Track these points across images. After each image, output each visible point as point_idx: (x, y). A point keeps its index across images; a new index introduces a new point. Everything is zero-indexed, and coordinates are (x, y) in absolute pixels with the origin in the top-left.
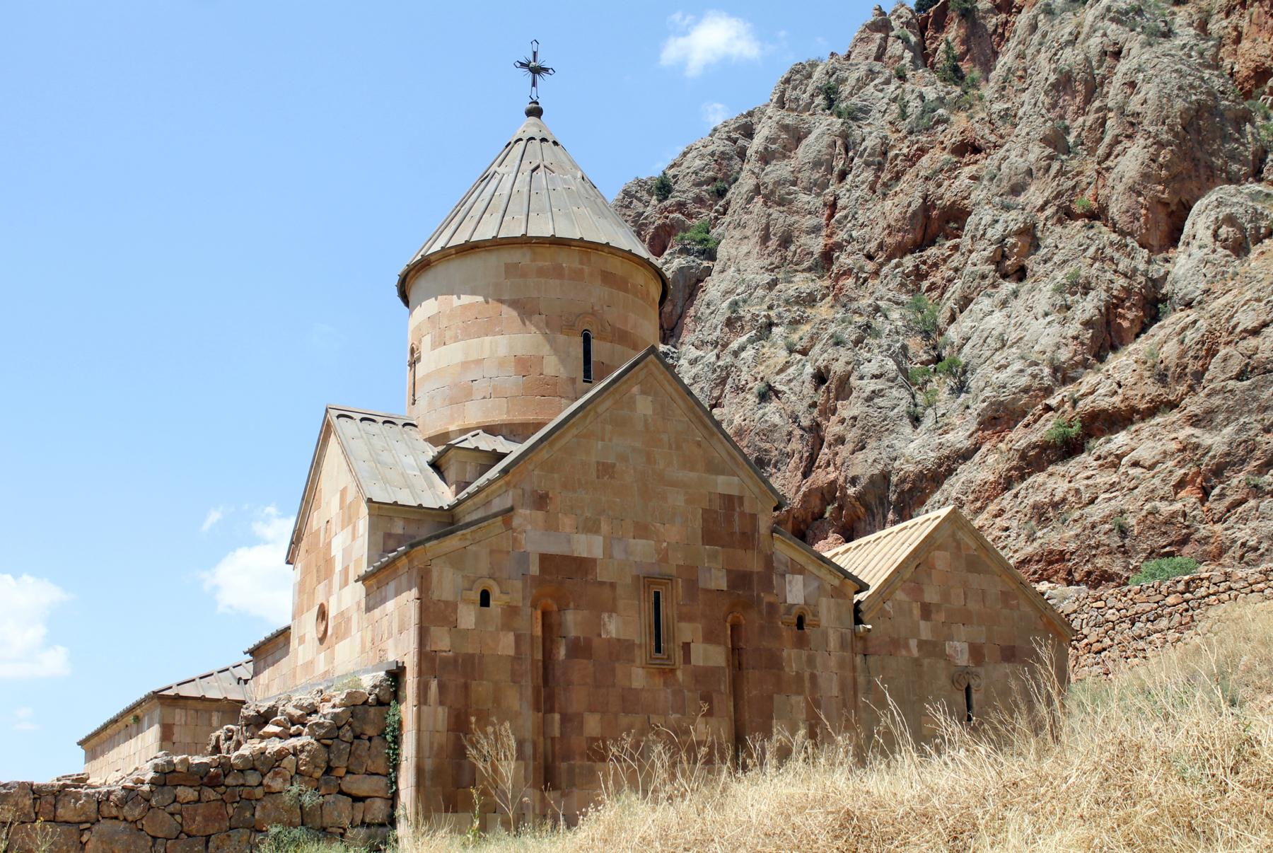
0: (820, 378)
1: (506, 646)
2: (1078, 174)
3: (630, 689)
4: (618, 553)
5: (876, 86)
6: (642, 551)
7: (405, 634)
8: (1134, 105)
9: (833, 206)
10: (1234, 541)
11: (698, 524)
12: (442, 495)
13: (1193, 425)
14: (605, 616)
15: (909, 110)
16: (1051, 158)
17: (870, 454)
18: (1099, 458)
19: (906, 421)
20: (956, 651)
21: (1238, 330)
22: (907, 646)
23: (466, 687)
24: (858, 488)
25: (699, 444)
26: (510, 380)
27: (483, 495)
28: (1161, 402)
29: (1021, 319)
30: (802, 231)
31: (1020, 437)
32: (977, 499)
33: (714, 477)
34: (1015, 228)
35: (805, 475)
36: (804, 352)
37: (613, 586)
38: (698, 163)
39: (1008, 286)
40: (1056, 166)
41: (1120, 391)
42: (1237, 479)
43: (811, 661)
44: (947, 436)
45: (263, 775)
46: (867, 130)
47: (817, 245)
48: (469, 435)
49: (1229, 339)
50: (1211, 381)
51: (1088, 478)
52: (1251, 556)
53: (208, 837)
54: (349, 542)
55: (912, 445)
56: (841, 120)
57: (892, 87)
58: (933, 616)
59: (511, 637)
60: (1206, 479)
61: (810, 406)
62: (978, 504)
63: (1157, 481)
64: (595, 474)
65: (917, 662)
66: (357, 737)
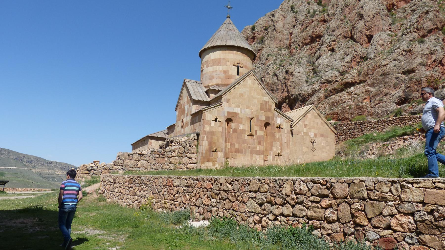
0: (287, 72)
1: (220, 129)
2: (348, 28)
3: (245, 139)
4: (243, 112)
5: (303, 6)
6: (248, 112)
7: (200, 126)
8: (362, 12)
9: (291, 34)
11: (259, 106)
12: (207, 99)
13: (369, 86)
14: (240, 124)
15: (310, 12)
16: (342, 24)
17: (297, 89)
18: (347, 92)
19: (305, 82)
20: (311, 134)
21: (381, 65)
22: (301, 133)
23: (212, 137)
24: (293, 97)
25: (260, 90)
26: (222, 75)
27: (216, 99)
28: (362, 81)
29: (332, 61)
30: (284, 39)
31: (330, 87)
32: (319, 100)
33: (263, 97)
34: (332, 40)
35: (282, 93)
36: (283, 66)
37: (242, 118)
38: (262, 23)
39: (330, 53)
40: (343, 26)
41: (353, 78)
42: (378, 98)
43: (281, 135)
44: (314, 86)
45: (172, 153)
46: (300, 16)
47: (287, 42)
48: (213, 86)
49: (379, 67)
50: (374, 76)
51: (344, 97)
52: (380, 115)
53: (161, 164)
54: (188, 107)
55: (306, 88)
56: (295, 14)
57: (306, 6)
58: (307, 127)
59: (221, 128)
60: (370, 98)
61: (284, 78)
62: (319, 101)
64: (239, 96)
65: (303, 136)
66: (190, 146)
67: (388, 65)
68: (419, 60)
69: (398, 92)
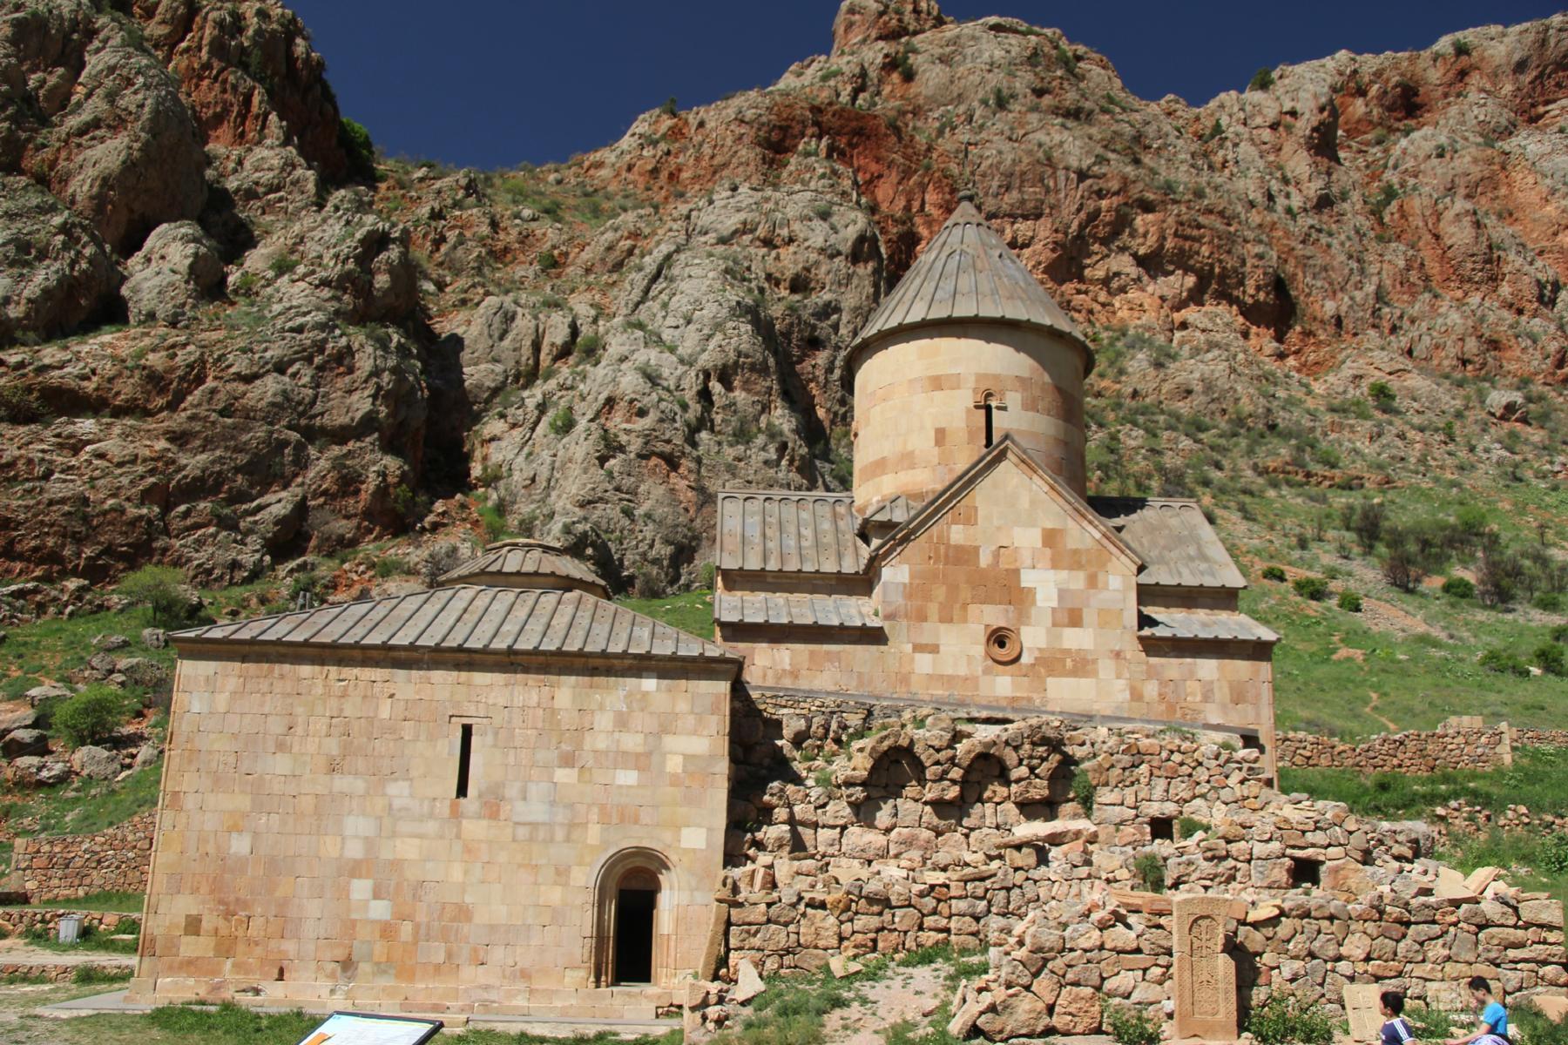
10: (189, 560)
13: (170, 440)
21: (233, 370)
28: (137, 406)
51: (43, 451)
63: (125, 481)
67: (258, 382)
68: (361, 404)
69: (279, 501)
